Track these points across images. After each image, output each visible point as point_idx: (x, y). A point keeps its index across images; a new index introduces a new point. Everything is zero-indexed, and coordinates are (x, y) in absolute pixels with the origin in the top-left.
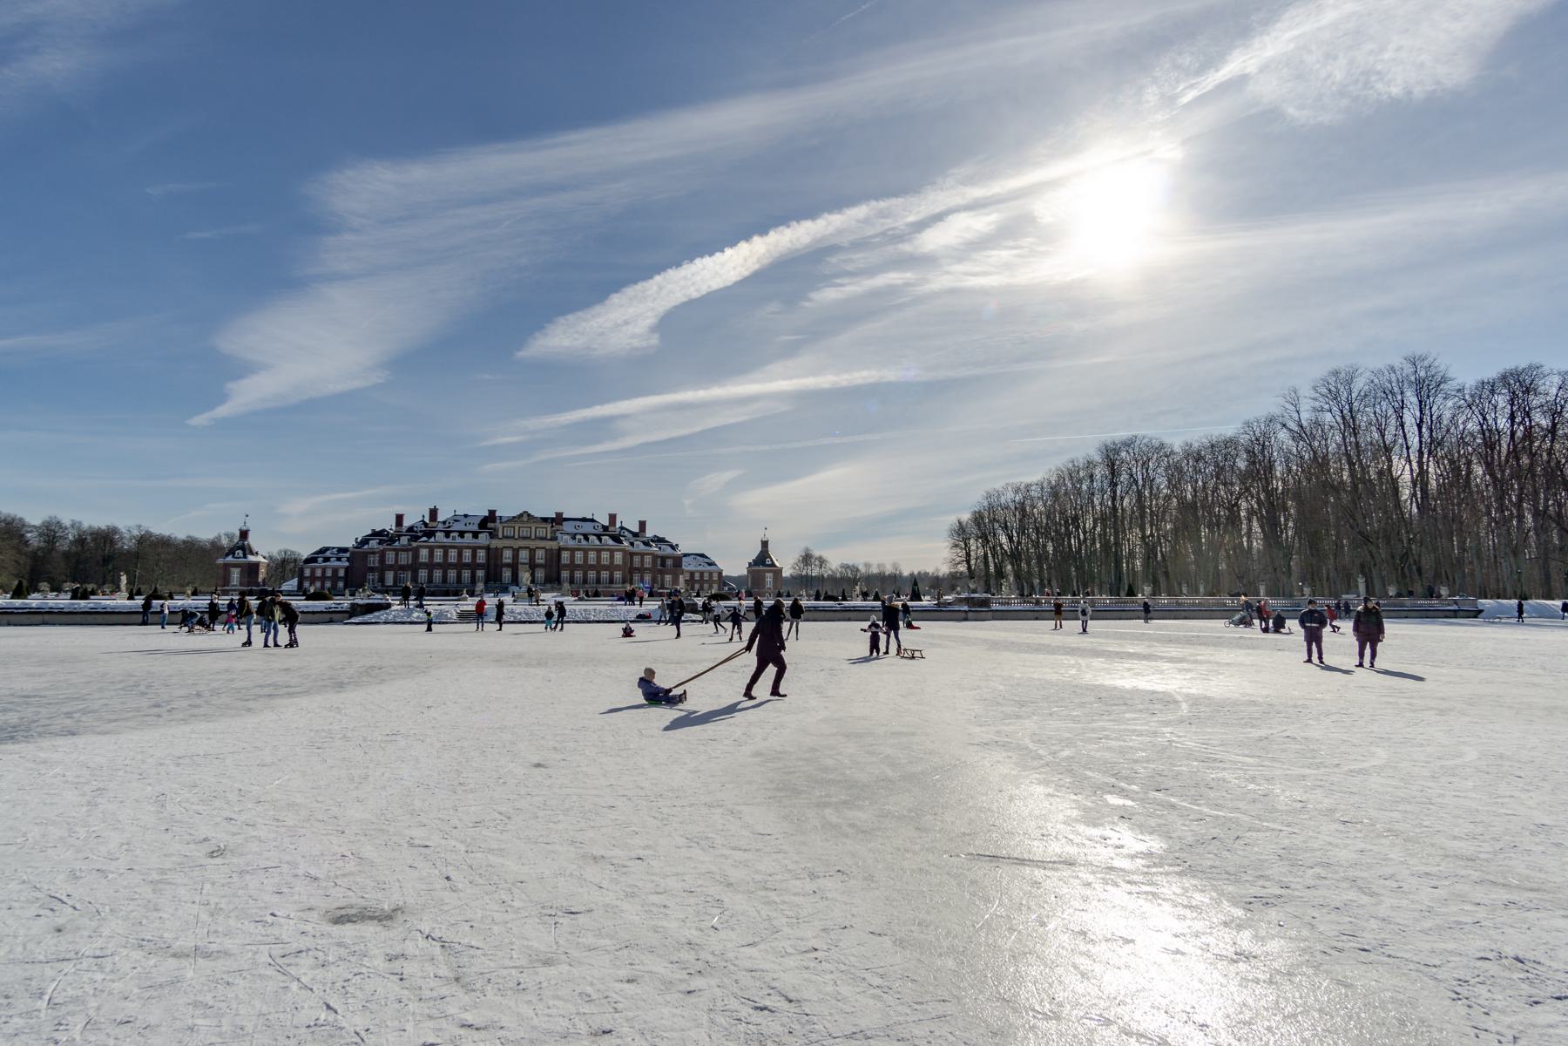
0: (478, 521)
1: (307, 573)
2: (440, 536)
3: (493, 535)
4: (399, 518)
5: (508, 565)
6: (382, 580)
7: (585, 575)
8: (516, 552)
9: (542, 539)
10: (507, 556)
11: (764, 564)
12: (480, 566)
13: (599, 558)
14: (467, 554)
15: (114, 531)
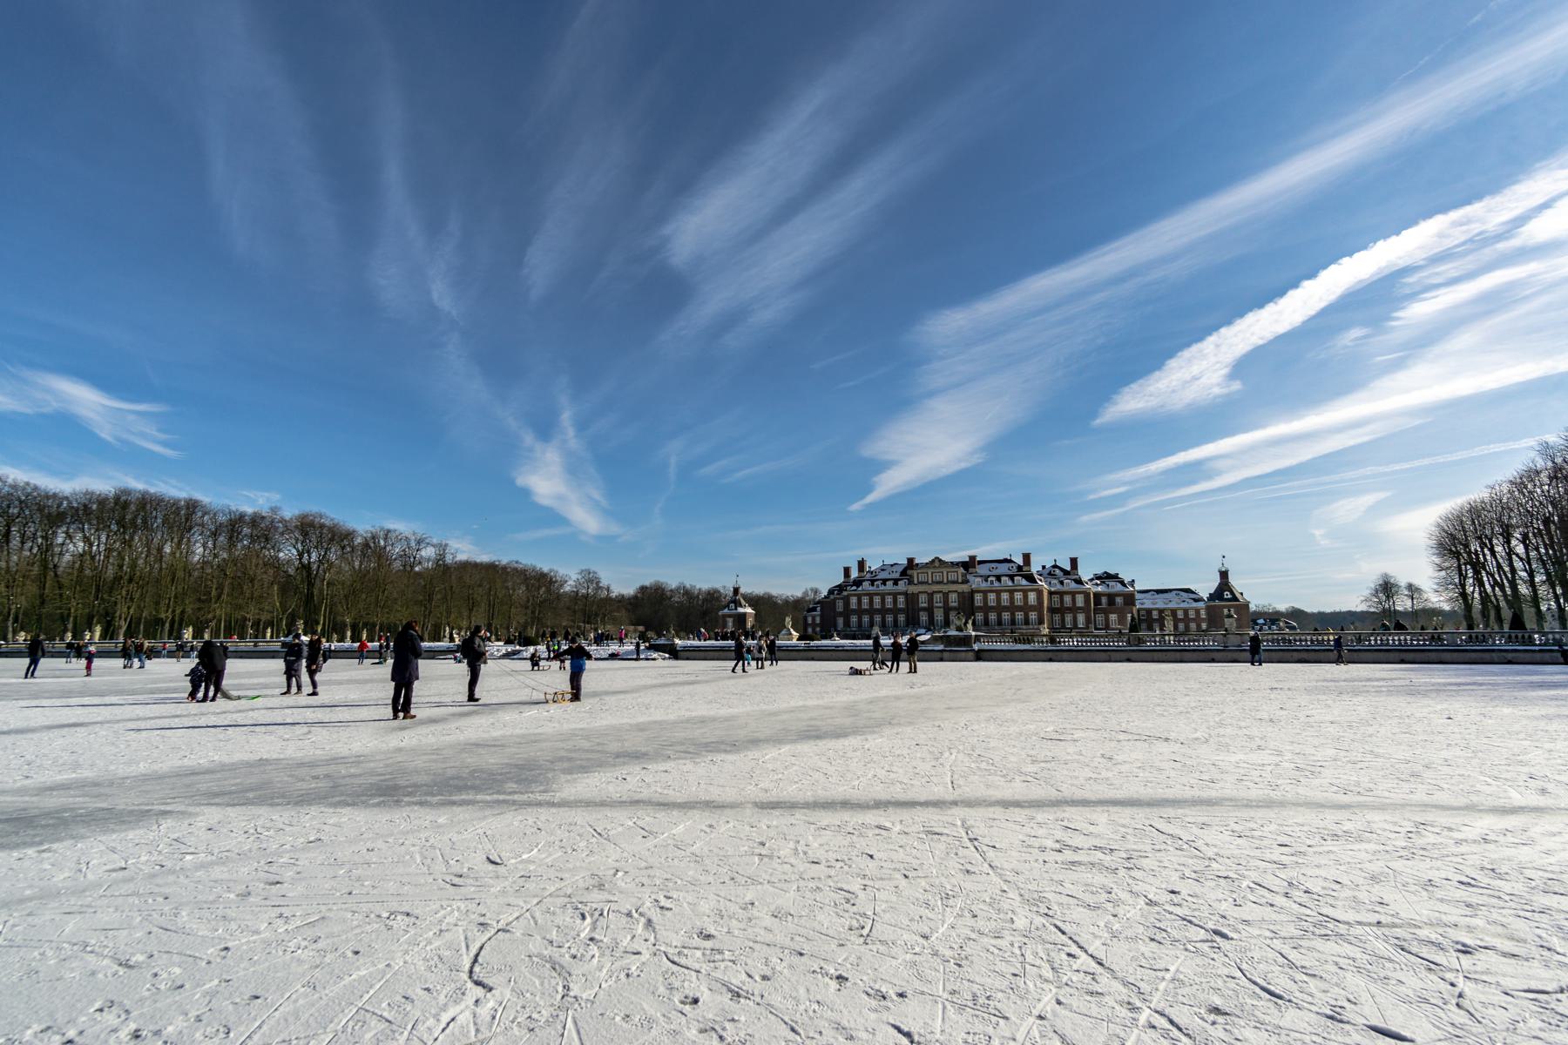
0: (900, 569)
1: (810, 620)
2: (866, 584)
3: (911, 582)
4: (847, 571)
5: (924, 609)
6: (847, 623)
7: (999, 617)
8: (931, 595)
9: (954, 582)
10: (923, 602)
11: (1221, 598)
12: (901, 610)
13: (1012, 599)
14: (889, 599)
15: (716, 591)
